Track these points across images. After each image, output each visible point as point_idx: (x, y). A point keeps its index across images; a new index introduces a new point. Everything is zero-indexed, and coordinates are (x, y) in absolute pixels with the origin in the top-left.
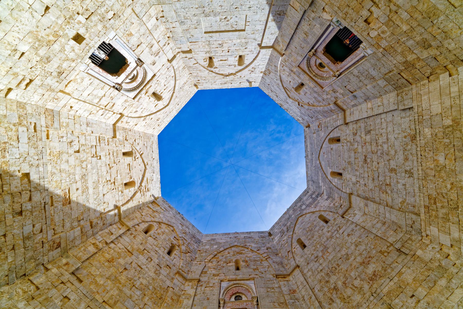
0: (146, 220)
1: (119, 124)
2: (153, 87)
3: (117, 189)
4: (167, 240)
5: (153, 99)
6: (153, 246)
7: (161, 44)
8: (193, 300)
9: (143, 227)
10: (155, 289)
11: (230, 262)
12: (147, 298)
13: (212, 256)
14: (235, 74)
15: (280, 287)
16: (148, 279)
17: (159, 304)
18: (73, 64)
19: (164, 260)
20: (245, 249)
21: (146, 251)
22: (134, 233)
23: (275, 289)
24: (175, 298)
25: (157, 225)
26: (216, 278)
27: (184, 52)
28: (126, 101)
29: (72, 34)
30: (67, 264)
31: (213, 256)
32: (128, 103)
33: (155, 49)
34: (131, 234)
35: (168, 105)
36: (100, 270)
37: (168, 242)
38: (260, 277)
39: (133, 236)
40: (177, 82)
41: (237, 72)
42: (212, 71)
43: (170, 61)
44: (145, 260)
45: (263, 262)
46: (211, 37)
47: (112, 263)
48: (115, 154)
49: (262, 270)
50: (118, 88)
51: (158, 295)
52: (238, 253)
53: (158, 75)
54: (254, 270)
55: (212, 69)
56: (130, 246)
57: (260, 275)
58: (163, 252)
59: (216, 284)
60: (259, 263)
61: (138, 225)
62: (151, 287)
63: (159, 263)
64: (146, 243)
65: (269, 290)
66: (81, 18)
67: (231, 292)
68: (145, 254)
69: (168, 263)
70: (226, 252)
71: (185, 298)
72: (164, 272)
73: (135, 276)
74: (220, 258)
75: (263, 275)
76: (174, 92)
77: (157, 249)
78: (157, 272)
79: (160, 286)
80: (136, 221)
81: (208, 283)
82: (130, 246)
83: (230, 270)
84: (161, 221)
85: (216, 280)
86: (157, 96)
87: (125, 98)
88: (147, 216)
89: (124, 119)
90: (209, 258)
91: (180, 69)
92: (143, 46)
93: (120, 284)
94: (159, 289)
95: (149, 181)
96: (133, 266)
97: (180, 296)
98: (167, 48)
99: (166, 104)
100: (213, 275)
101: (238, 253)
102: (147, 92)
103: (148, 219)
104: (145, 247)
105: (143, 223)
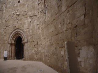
29: (19, 4)
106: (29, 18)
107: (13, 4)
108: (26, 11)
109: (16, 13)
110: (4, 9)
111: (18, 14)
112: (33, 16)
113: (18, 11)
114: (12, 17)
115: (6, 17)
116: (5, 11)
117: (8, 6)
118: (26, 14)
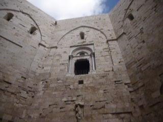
1: (116, 38)
2: (78, 41)
5: (85, 37)
7: (52, 58)
14: (21, 11)
18: (95, 76)
27: (45, 46)
28: (97, 46)
29: (81, 86)
32: (98, 44)
33: (58, 58)
35: (83, 26)
40: (64, 34)
41: (18, 11)
42: (37, 25)
43: (56, 47)
46: (19, 42)
48: (135, 23)
50: (93, 55)
53: (69, 46)
55: (35, 25)
66: (71, 87)
76: (72, 31)
86: (82, 36)
87: (96, 48)
89: (109, 38)
91: (55, 40)
92: (61, 63)
98: (51, 54)
99: (82, 28)
102: (84, 42)
106: (110, 115)
107: (67, 84)
108: (100, 101)
109: (73, 101)
110: (40, 89)
111: (82, 103)
112: (121, 113)
113: (80, 98)
114: (61, 108)
115: (42, 107)
116: (41, 94)
117: (52, 86)
118: (104, 107)
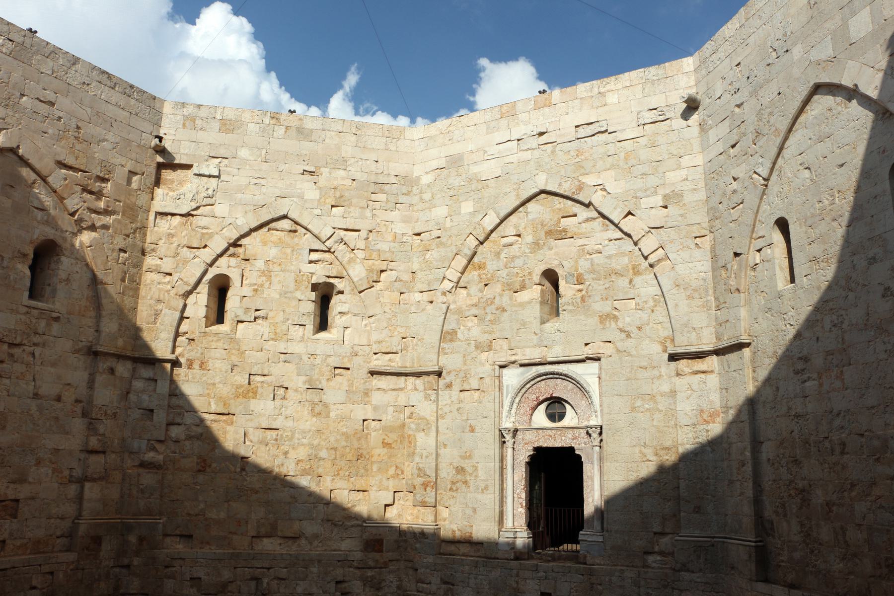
0: (193, 281)
3: (36, 339)
4: (292, 286)
6: (267, 346)
8: (437, 432)
9: (202, 312)
10: (335, 449)
11: (523, 287)
12: (329, 479)
13: (461, 262)
15: (673, 393)
16: (305, 441)
17: (362, 471)
19: (318, 361)
20: (577, 209)
21: (259, 379)
22: (192, 355)
23: (659, 398)
24: (392, 437)
25: (233, 261)
26: (484, 356)
30: (141, 539)
31: (464, 262)
34: (190, 365)
36: (201, 498)
37: (298, 295)
38: (618, 351)
39: (196, 366)
44: (270, 404)
45: (638, 280)
47: (208, 470)
49: (627, 320)
51: (349, 457)
52: (549, 233)
54: (605, 318)
56: (213, 402)
57: (619, 345)
58: (303, 340)
59: (487, 380)
60: (623, 282)
61: (182, 318)
62: (323, 454)
63: (310, 381)
64: (242, 353)
65: (639, 403)
67: (532, 397)
68: (260, 390)
69: (334, 361)
70: (508, 228)
71: (418, 430)
72: (335, 393)
73: (275, 456)
74: (492, 266)
75: (629, 344)
77: (282, 347)
78: (318, 409)
79: (343, 434)
80: (170, 317)
81: (465, 378)
82: (213, 402)
83: (524, 324)
84: (235, 235)
85: (485, 364)
88: (185, 262)
90: (453, 274)
93: (257, 492)
94: (344, 443)
95: (70, 161)
96: (255, 439)
97: (403, 425)
100: (477, 347)
101: (549, 233)
103: (192, 272)
104: (248, 371)
105: (191, 299)
